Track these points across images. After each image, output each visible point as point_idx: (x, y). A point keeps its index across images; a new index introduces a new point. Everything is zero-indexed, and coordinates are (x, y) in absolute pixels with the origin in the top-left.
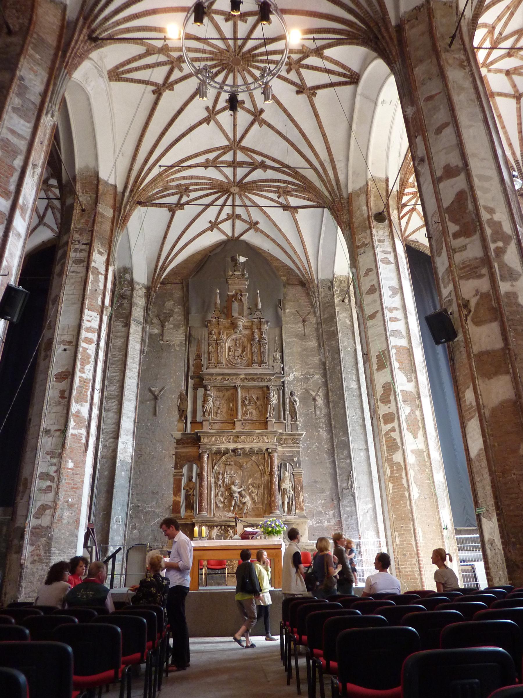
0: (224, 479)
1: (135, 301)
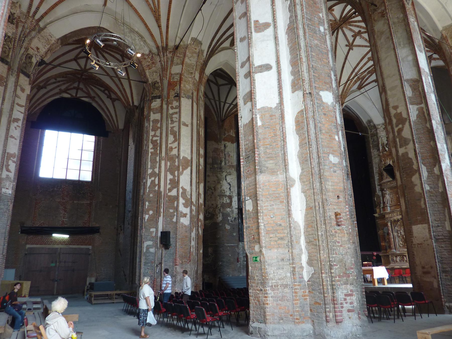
0: (401, 233)
1: (379, 135)
